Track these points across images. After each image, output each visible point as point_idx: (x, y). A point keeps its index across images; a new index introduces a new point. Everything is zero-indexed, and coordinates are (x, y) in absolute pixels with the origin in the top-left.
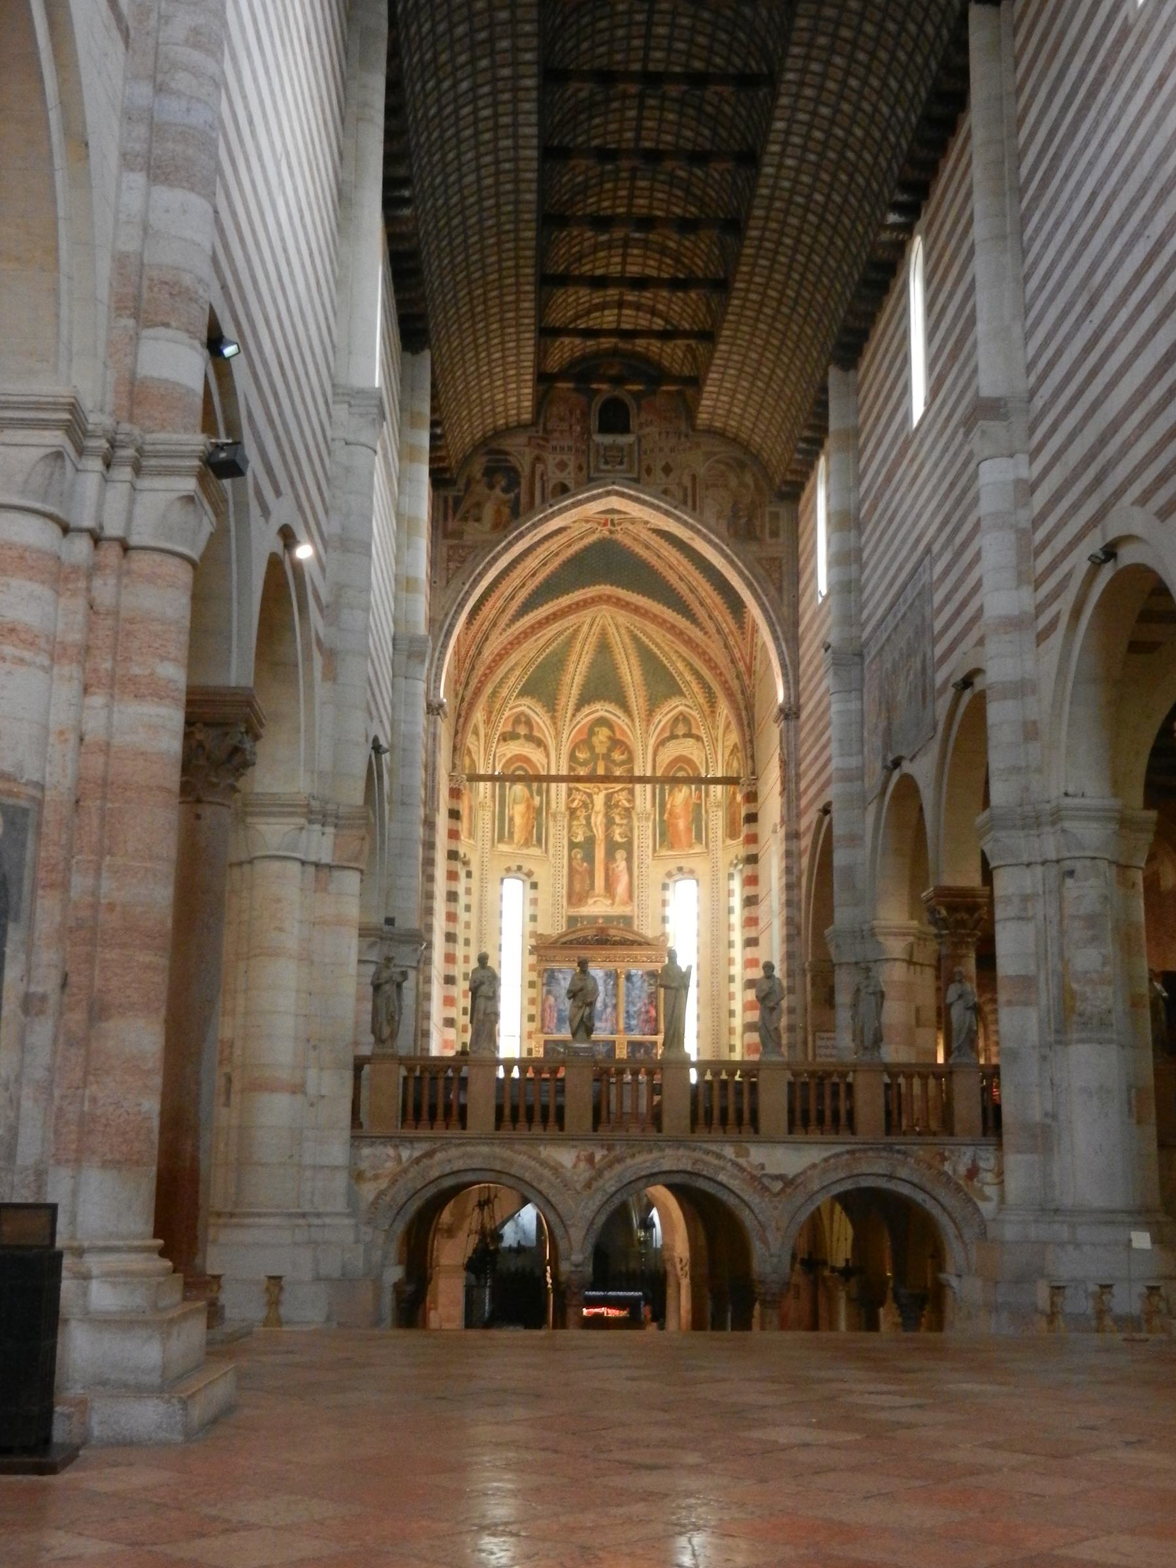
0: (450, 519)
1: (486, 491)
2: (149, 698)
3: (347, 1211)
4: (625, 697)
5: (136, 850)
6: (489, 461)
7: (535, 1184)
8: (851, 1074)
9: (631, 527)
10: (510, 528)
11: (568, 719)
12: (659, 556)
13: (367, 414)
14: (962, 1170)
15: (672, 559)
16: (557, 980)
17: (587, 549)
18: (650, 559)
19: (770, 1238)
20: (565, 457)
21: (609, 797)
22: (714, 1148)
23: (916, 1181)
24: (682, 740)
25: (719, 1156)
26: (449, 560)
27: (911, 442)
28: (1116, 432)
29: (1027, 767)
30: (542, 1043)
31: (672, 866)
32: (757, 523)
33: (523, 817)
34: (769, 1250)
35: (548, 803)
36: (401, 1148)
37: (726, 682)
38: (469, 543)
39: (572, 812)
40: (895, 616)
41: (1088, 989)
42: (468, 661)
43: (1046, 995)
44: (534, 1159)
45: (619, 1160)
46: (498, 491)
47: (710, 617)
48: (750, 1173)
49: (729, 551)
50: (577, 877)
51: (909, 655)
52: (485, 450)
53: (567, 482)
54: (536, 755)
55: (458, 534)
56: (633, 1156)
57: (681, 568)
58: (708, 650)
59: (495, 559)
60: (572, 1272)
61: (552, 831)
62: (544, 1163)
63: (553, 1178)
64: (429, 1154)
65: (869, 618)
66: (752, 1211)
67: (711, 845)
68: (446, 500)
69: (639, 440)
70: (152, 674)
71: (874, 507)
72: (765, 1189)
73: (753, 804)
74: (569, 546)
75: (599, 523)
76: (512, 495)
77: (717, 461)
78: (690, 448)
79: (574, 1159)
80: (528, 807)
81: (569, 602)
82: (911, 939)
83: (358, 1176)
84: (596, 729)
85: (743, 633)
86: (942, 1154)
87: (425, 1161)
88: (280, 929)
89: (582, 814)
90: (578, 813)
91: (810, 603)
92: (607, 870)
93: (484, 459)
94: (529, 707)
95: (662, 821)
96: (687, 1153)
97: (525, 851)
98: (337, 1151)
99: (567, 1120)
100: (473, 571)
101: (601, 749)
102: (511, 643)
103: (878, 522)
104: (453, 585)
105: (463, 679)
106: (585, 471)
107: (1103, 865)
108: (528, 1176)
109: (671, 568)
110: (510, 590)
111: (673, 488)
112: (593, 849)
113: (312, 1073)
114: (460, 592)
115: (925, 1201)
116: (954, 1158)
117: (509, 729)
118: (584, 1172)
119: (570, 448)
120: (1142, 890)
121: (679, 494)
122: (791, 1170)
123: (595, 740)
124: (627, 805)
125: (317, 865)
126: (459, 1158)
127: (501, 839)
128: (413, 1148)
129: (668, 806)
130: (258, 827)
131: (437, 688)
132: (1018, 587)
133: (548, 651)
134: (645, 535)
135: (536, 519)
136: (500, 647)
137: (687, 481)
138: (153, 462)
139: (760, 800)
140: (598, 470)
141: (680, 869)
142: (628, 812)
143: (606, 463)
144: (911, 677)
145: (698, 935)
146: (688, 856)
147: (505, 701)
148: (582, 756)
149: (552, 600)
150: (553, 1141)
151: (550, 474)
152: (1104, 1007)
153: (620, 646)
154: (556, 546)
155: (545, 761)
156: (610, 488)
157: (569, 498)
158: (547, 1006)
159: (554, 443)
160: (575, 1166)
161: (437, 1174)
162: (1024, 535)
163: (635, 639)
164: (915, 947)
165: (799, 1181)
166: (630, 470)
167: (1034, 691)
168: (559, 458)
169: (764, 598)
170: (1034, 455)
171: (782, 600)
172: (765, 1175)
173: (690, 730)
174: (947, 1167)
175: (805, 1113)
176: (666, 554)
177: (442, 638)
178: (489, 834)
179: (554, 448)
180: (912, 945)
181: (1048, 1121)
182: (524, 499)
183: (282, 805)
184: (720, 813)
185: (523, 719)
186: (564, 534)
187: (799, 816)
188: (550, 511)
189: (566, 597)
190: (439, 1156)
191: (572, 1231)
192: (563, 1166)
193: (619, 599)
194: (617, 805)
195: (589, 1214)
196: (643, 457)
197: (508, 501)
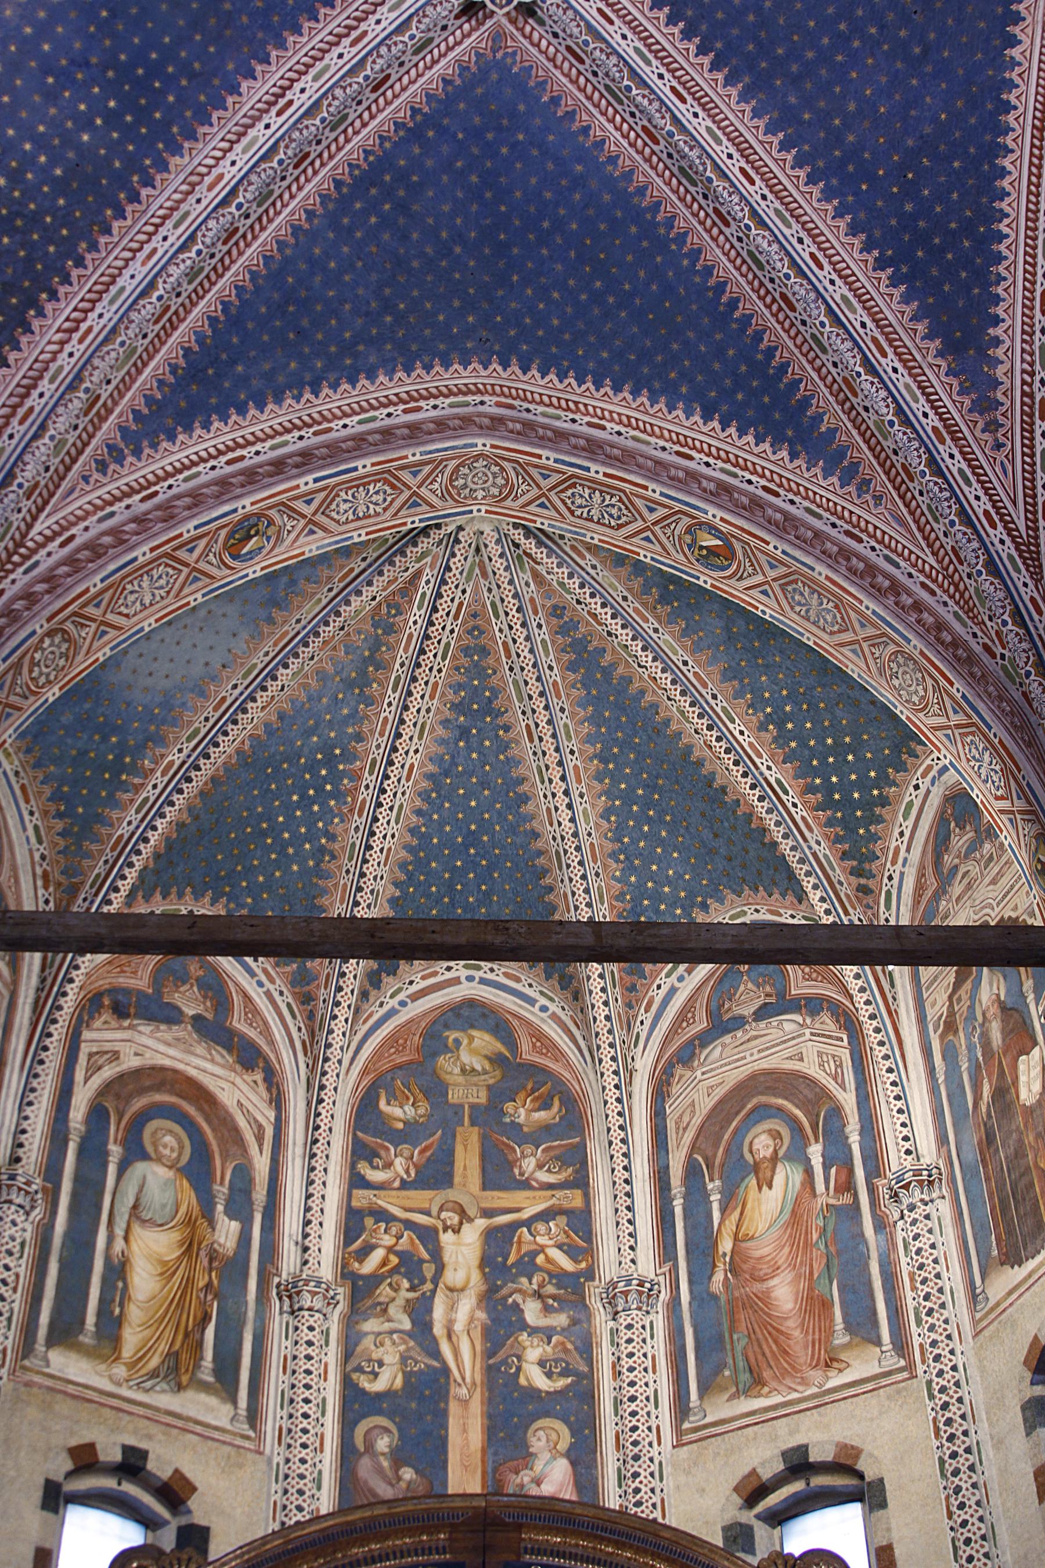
24: (754, 1029)
33: (167, 1272)
35: (270, 1251)
37: (940, 626)
61: (278, 1347)
67: (917, 1336)
80: (190, 1247)
85: (992, 426)
90: (384, 1291)
95: (702, 1298)
97: (165, 1400)
112: (441, 1416)
124: (566, 1264)
129: (726, 1245)
146: (824, 1400)
155: (267, 1116)
173: (782, 994)
184: (944, 1209)
194: (528, 1265)
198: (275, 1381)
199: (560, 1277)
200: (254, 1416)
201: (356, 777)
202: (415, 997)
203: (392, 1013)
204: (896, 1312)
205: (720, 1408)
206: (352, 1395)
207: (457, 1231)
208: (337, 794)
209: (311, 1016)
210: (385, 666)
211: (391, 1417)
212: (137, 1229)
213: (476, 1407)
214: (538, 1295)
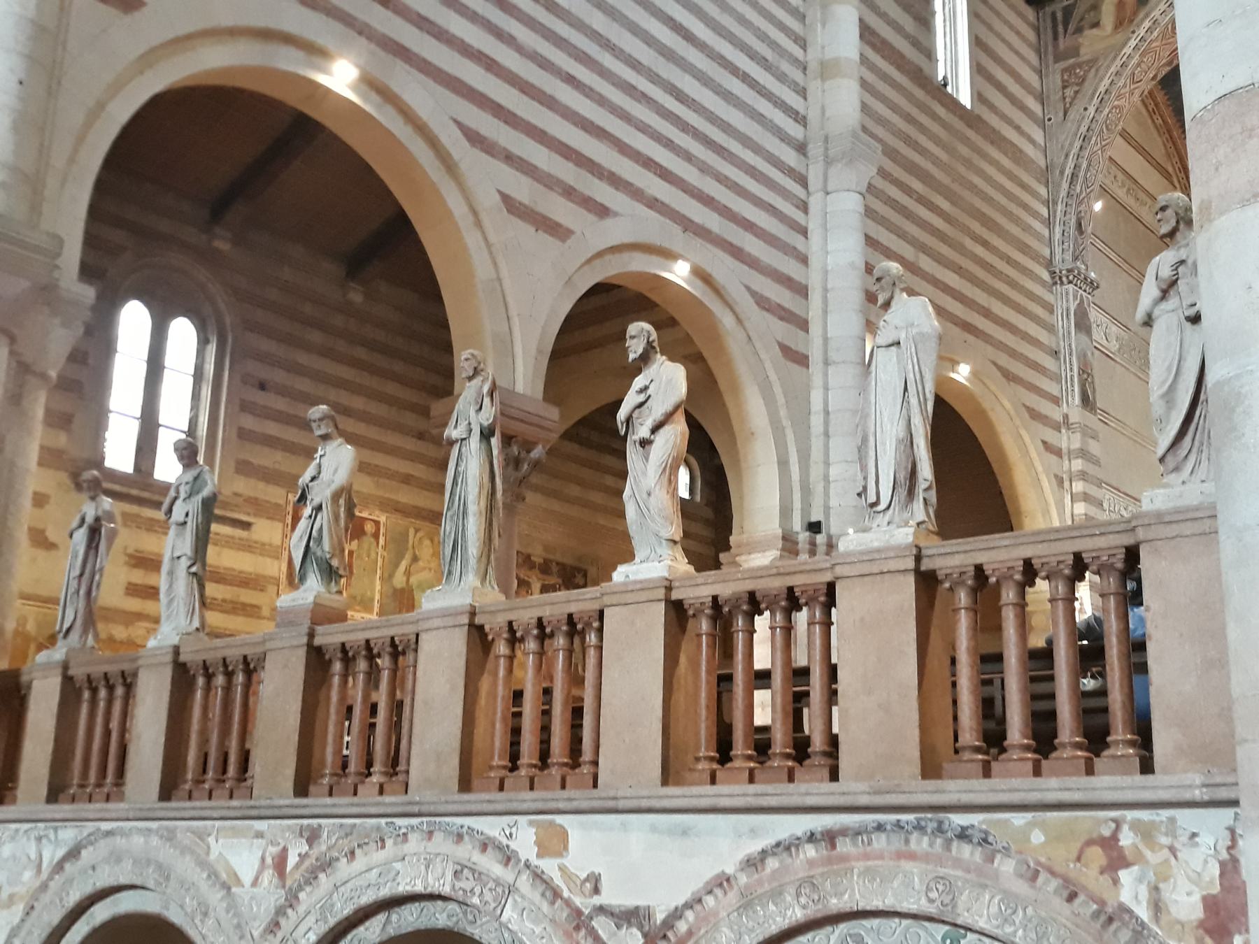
22: (492, 827)
26: (1064, 87)
55: (1075, 51)
68: (1054, 15)
86: (1109, 844)
100: (1095, 91)
104: (1072, 115)
116: (1153, 857)
160: (255, 883)
172: (601, 910)
177: (1065, 186)
192: (239, 882)
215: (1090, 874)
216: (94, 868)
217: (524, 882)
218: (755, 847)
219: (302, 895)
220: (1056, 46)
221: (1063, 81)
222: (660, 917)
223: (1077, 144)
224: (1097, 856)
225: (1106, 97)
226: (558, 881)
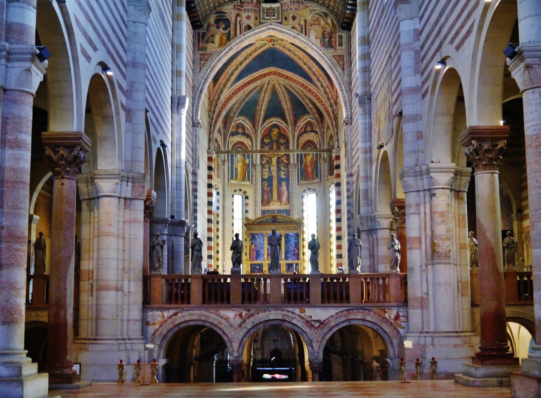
0: (201, 43)
1: (216, 30)
2: (15, 148)
3: (143, 337)
4: (285, 115)
5: (12, 206)
6: (217, 17)
7: (218, 325)
8: (348, 278)
9: (282, 42)
10: (226, 46)
11: (260, 125)
12: (295, 55)
13: (142, 10)
14: (393, 316)
15: (300, 55)
16: (256, 238)
17: (264, 52)
18: (291, 56)
19: (315, 345)
20: (250, 14)
21: (278, 159)
22: (291, 309)
23: (373, 321)
24: (309, 133)
25: (293, 313)
26: (201, 60)
27: (385, 8)
28: (444, 12)
29: (418, 150)
30: (250, 265)
31: (305, 188)
32: (333, 40)
33: (241, 168)
34: (313, 349)
36: (164, 312)
37: (326, 108)
38: (209, 53)
39: (263, 166)
40: (381, 83)
41: (441, 242)
42: (214, 102)
43: (425, 245)
44: (218, 316)
45: (252, 315)
46: (221, 29)
47: (318, 80)
48: (306, 320)
49: (321, 53)
50: (266, 193)
51: (385, 101)
52: (215, 12)
53: (250, 25)
54: (247, 141)
55: (205, 49)
56: (258, 314)
57: (305, 59)
58: (318, 95)
59: (220, 59)
60: (234, 360)
61: (254, 174)
62: (222, 317)
63: (225, 323)
64: (175, 314)
65: (373, 83)
66: (307, 335)
67: (322, 178)
68: (199, 34)
69: (282, 5)
70: (16, 138)
71: (374, 35)
72: (312, 326)
73: (338, 161)
74: (256, 51)
75: (268, 41)
76: (227, 31)
77: (316, 14)
78: (304, 8)
79: (234, 315)
80: (243, 164)
81: (257, 75)
82: (391, 220)
83: (145, 323)
84: (273, 129)
86: (384, 310)
87: (174, 317)
88: (110, 225)
89: (267, 166)
90: (265, 166)
91: (355, 75)
92: (278, 190)
93: (215, 15)
94: (243, 120)
95: (301, 168)
96: (280, 312)
97: (243, 183)
98: (136, 313)
99: (231, 299)
100: (211, 65)
101: (275, 138)
102: (233, 94)
103: (375, 43)
105: (212, 110)
106: (258, 20)
107: (449, 191)
108: (215, 323)
109: (300, 59)
110: (231, 71)
111: (297, 26)
113: (126, 283)
114: (205, 74)
115: (377, 329)
116: (389, 312)
117: (234, 130)
118: (238, 320)
119: (252, 10)
120: (466, 200)
121: (299, 28)
122: (322, 319)
123: (272, 134)
124: (286, 162)
125: (125, 199)
126: (187, 315)
127: (232, 178)
128: (169, 312)
129: (304, 162)
130: (100, 183)
131: (197, 116)
132: (415, 75)
133: (250, 96)
134: (288, 46)
135: (237, 41)
136: (228, 96)
137: (302, 23)
138: (14, 56)
139: (341, 159)
140: (264, 19)
141: (309, 189)
142: (287, 165)
143: (268, 16)
144: (386, 110)
145: (317, 217)
146: (313, 183)
147: (232, 118)
148: (266, 141)
149: (250, 74)
150: (226, 308)
151: (243, 21)
152: (447, 249)
153: (281, 93)
154: (250, 51)
155: (250, 144)
156: (269, 27)
157: (252, 31)
158: (251, 248)
159: (245, 8)
160: (234, 318)
161: (179, 322)
162: (417, 53)
163: (287, 90)
164: (394, 224)
165: (326, 322)
166: (277, 19)
167: (421, 119)
168: (247, 14)
169: (337, 73)
170: (421, 18)
171: (344, 73)
172: (312, 320)
173: (313, 129)
174: (387, 315)
175: (329, 294)
176: (298, 53)
178: (227, 176)
179: (245, 10)
180: (392, 222)
181: (425, 296)
182: (232, 33)
183: (109, 175)
184: (326, 165)
185: (240, 126)
186: (253, 46)
187: (353, 166)
188: (244, 37)
189: (256, 73)
190: (180, 315)
191: (233, 344)
192: (230, 318)
193: (279, 73)
194: (282, 162)
195: (240, 337)
196: (283, 12)
197: (225, 34)
198: (254, 178)
199: (285, 163)
200: (252, 183)
201: (259, 102)
202: (268, 124)
203: (265, 126)
204: (320, 175)
205: (302, 182)
206: (262, 178)
207: (274, 157)
208: (257, 104)
209: (255, 130)
210: (262, 90)
211: (267, 181)
212: (238, 163)
213: (276, 180)
214: (283, 166)
215: (382, 314)
216: (184, 317)
217: (297, 317)
218: (337, 311)
219: (247, 320)
220: (199, 46)
221: (200, 58)
222: (322, 321)
223: (203, 81)
224: (383, 312)
225: (214, 68)
226: (304, 316)
